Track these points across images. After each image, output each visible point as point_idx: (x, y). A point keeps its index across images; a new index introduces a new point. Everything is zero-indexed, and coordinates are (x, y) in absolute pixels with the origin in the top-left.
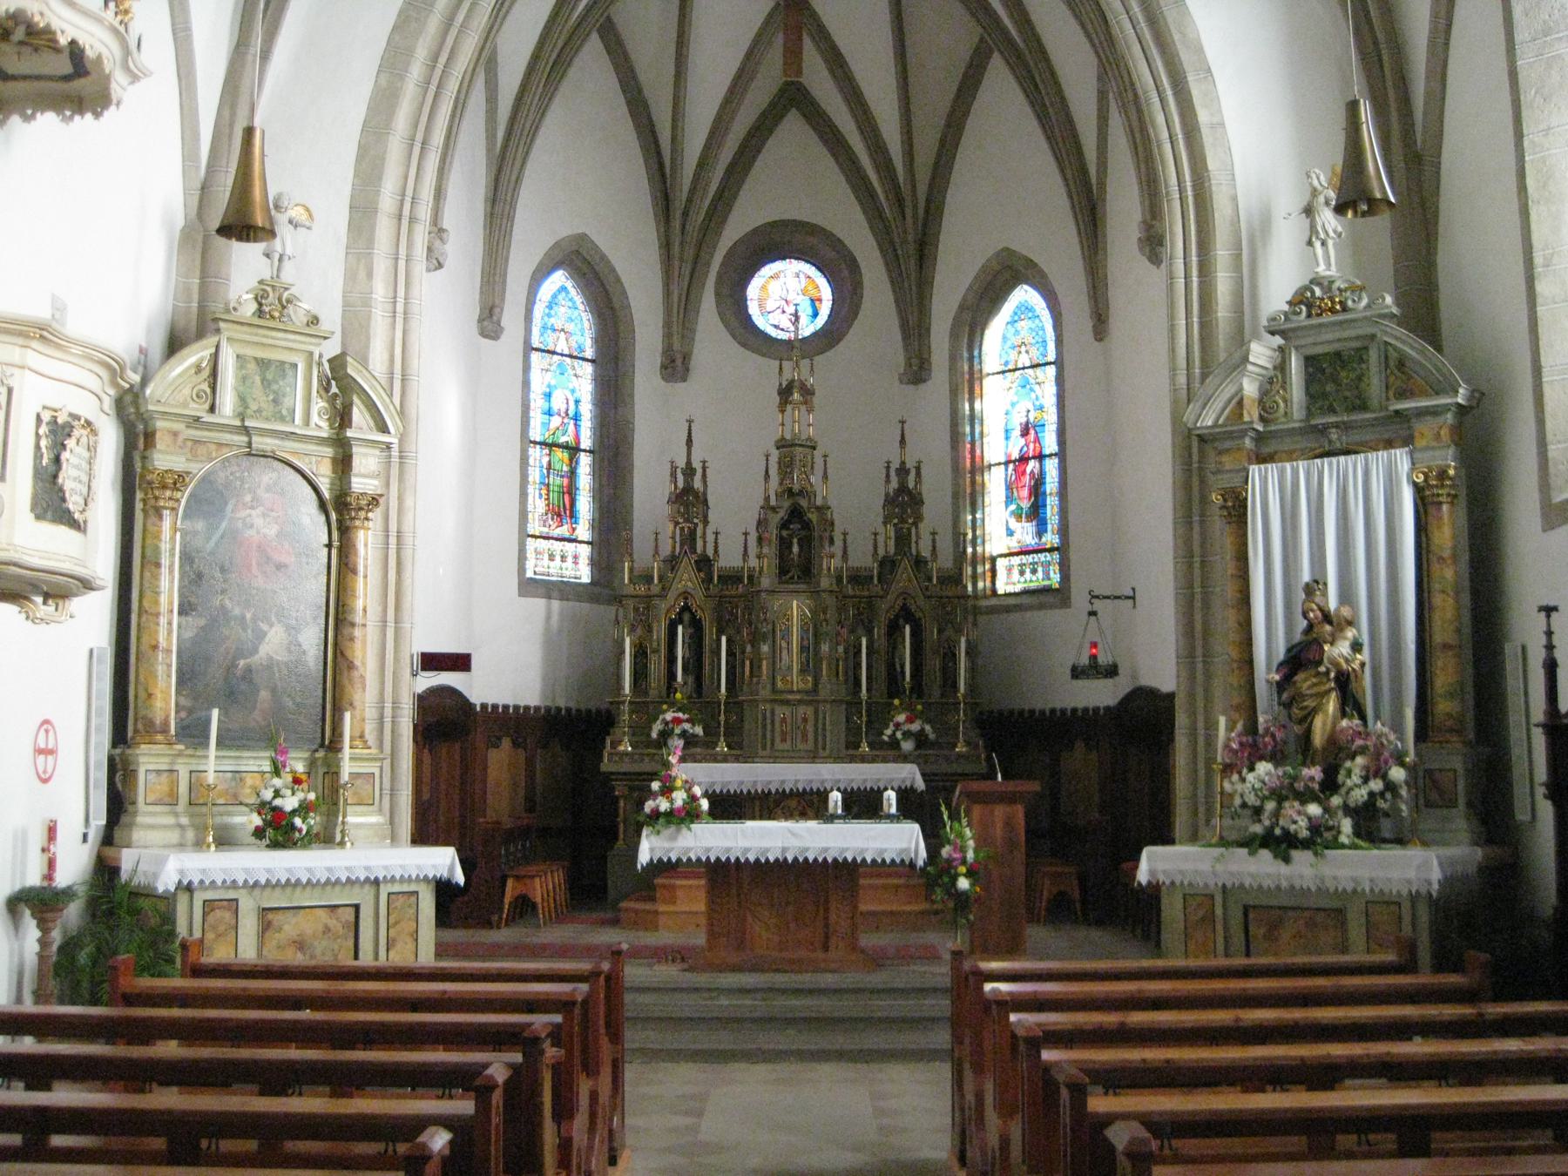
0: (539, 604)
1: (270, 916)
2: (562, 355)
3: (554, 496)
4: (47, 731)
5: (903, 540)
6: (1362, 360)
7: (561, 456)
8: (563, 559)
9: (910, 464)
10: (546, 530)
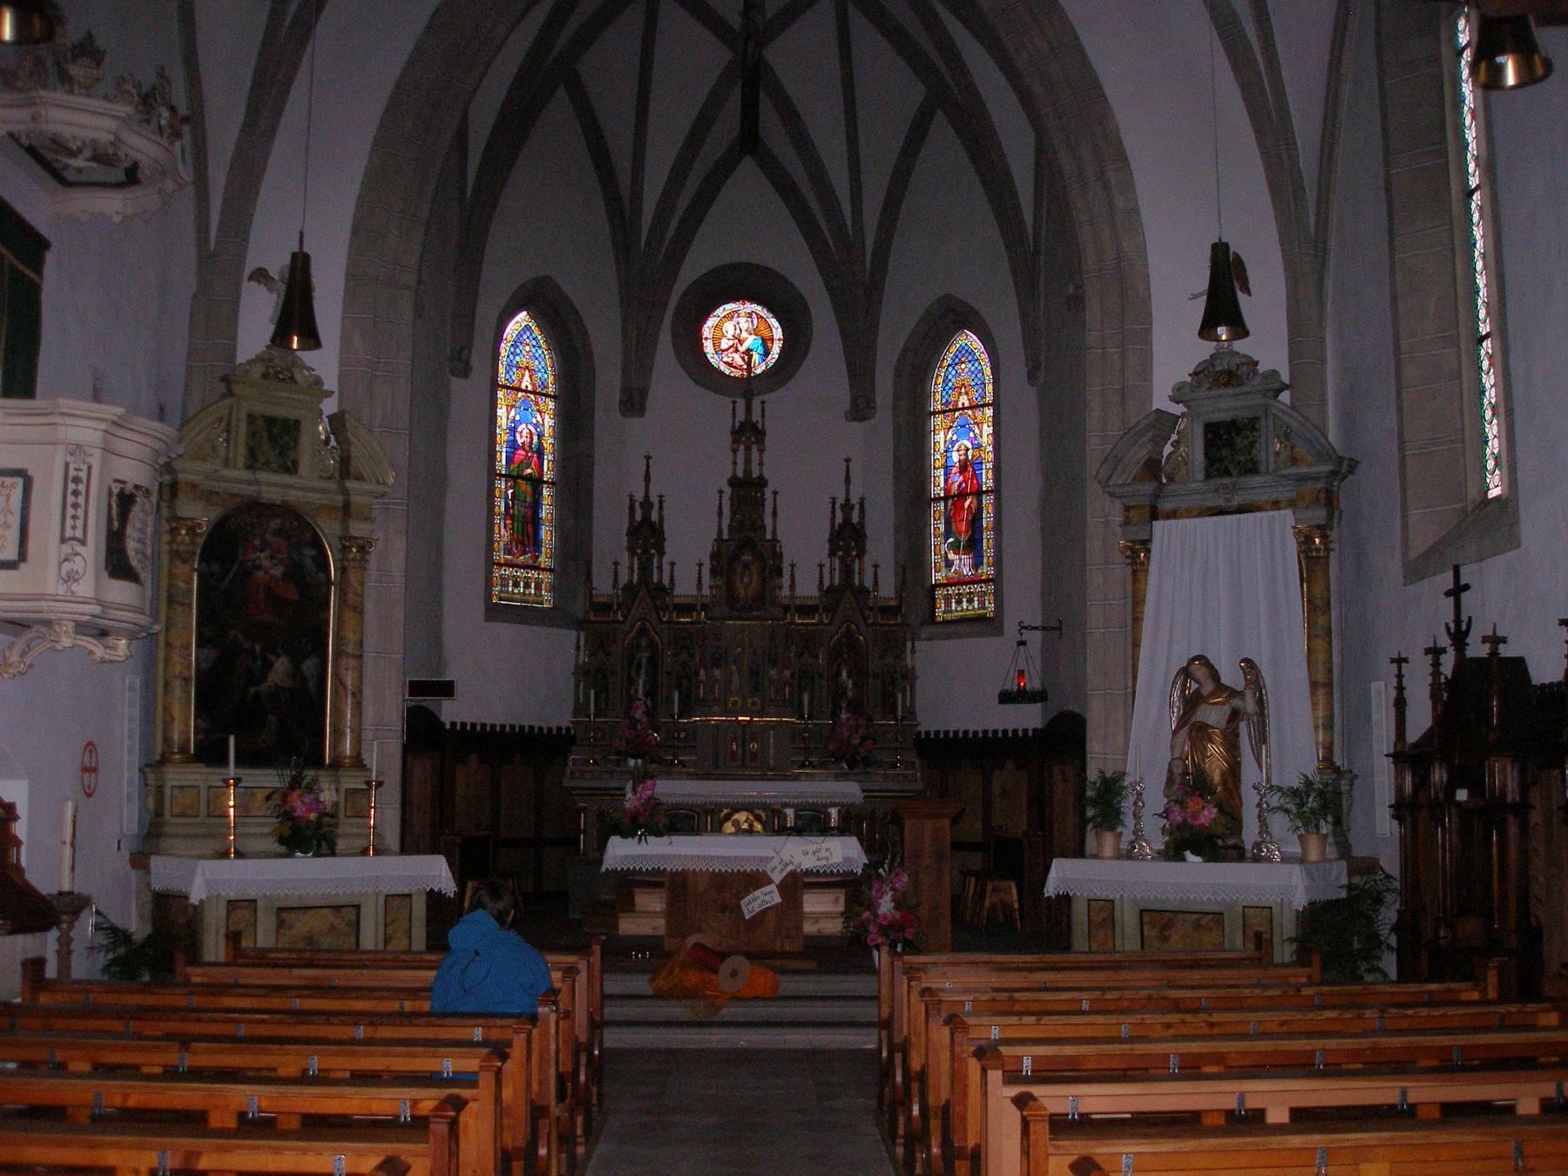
0: (507, 631)
1: (284, 915)
4: (91, 752)
5: (847, 571)
6: (1254, 429)
7: (525, 487)
8: (527, 586)
9: (855, 500)
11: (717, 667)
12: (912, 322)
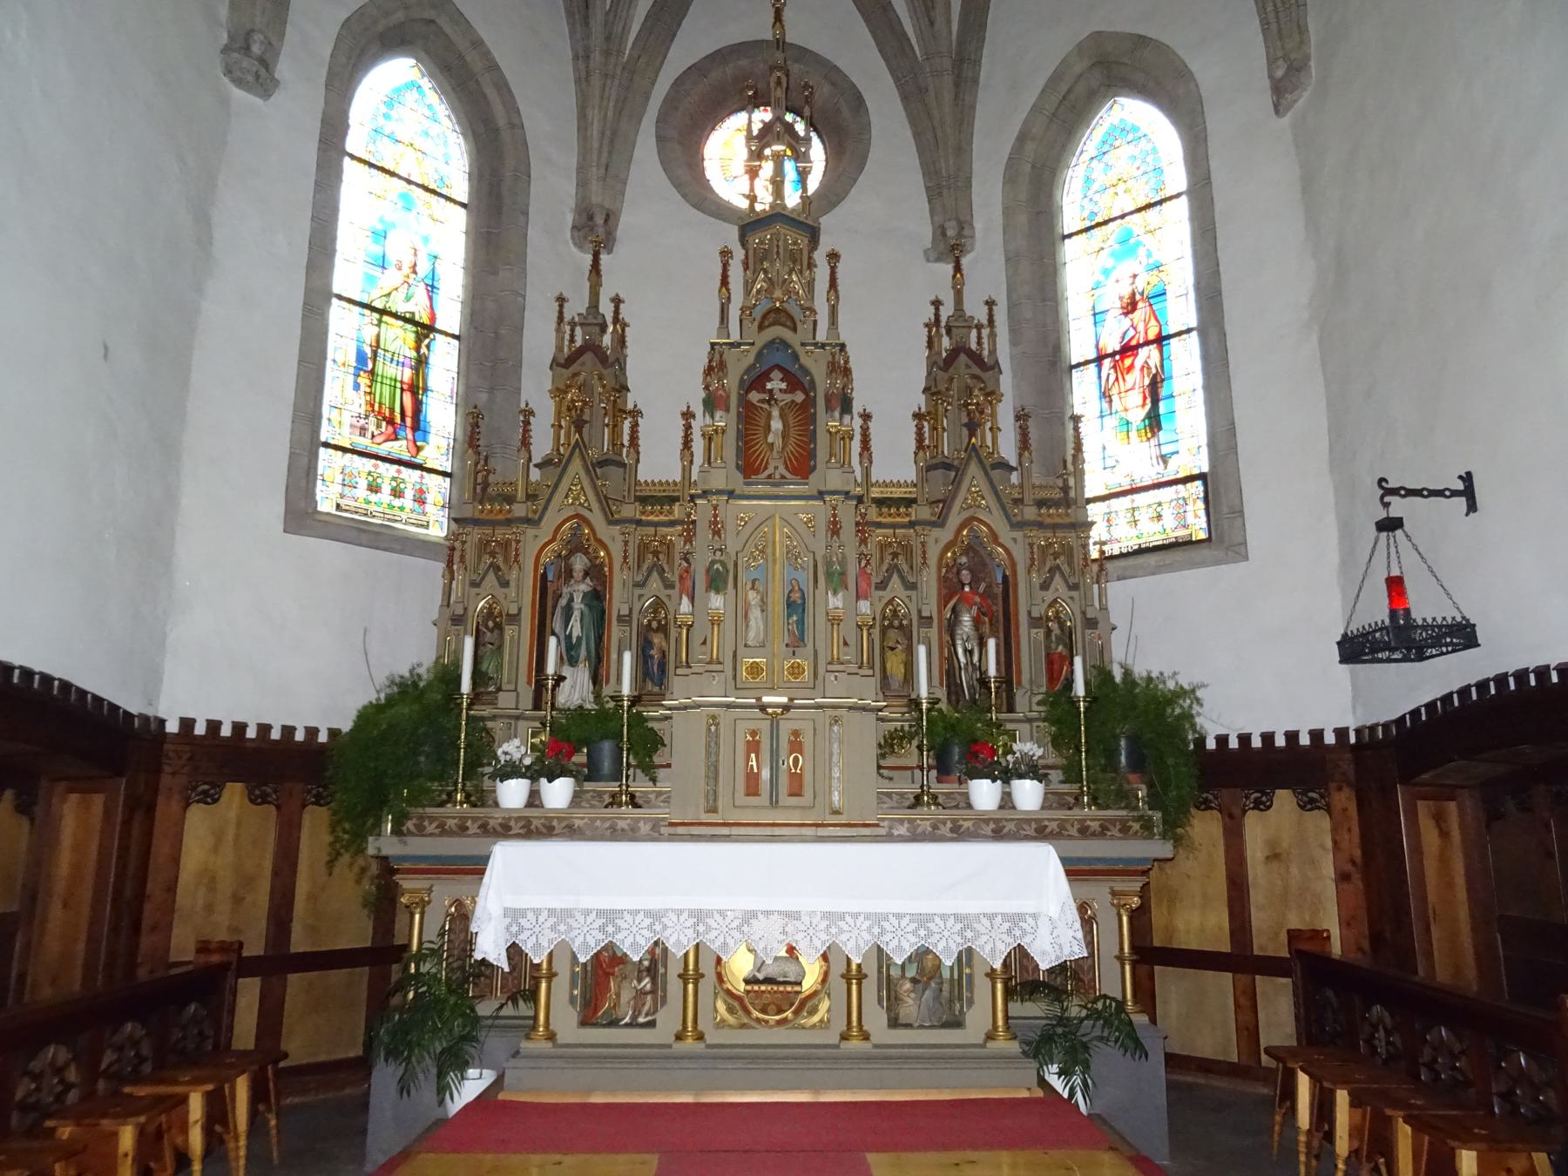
2: (409, 182)
3: (384, 392)
7: (399, 339)
8: (397, 493)
10: (364, 443)
11: (718, 591)
12: (1031, 96)
